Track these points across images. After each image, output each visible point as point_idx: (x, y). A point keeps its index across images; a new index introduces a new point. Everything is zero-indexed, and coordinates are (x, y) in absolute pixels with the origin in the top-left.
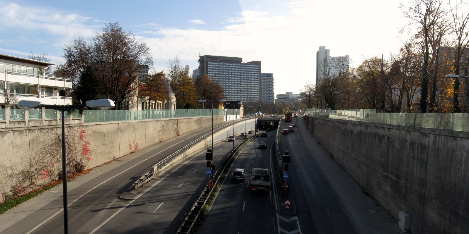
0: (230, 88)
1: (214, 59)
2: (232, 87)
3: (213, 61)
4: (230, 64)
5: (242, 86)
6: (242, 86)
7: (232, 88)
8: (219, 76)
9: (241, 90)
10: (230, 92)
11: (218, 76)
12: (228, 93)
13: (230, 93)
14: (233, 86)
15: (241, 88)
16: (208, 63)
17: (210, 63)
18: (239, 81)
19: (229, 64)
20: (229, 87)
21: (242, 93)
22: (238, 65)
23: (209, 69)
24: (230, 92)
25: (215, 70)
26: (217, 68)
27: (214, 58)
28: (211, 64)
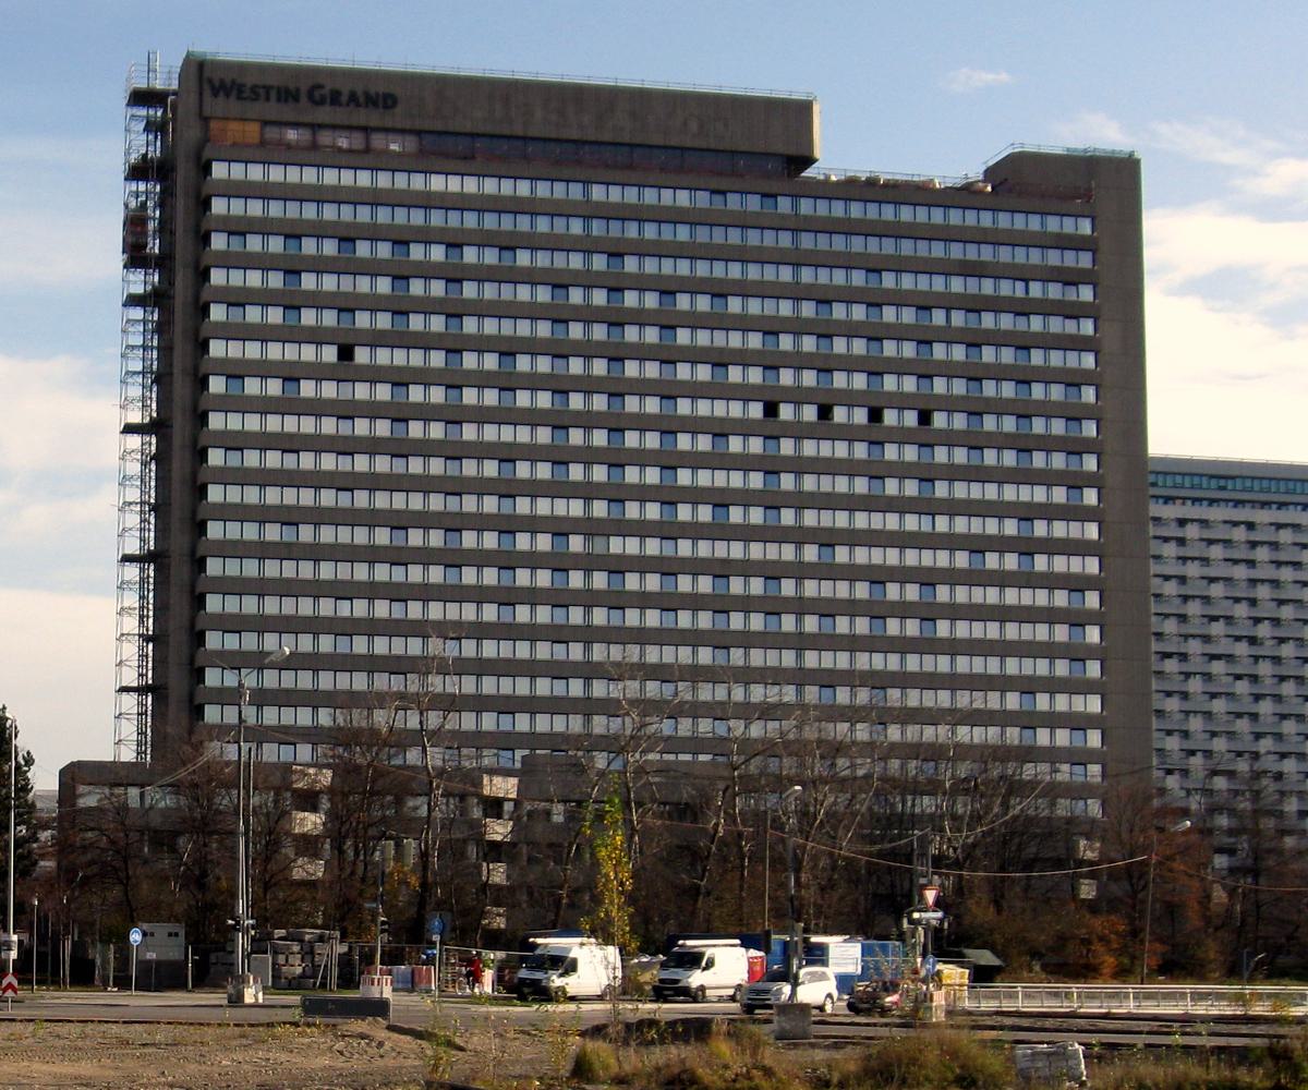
0: (588, 564)
1: (324, 114)
2: (632, 546)
3: (314, 146)
4: (598, 193)
5: (799, 536)
6: (799, 536)
7: (618, 566)
8: (400, 379)
9: (788, 588)
10: (599, 616)
11: (374, 375)
12: (559, 634)
13: (588, 635)
14: (642, 530)
15: (788, 552)
16: (219, 170)
17: (237, 171)
18: (756, 445)
19: (576, 191)
20: (576, 543)
21: (801, 642)
22: (733, 201)
23: (229, 261)
24: (599, 616)
25: (329, 283)
26: (363, 249)
27: (335, 98)
28: (265, 192)
